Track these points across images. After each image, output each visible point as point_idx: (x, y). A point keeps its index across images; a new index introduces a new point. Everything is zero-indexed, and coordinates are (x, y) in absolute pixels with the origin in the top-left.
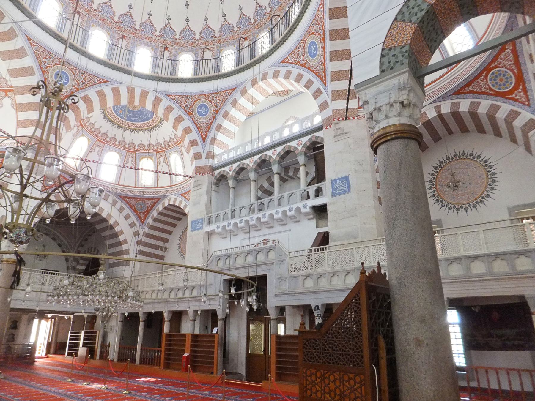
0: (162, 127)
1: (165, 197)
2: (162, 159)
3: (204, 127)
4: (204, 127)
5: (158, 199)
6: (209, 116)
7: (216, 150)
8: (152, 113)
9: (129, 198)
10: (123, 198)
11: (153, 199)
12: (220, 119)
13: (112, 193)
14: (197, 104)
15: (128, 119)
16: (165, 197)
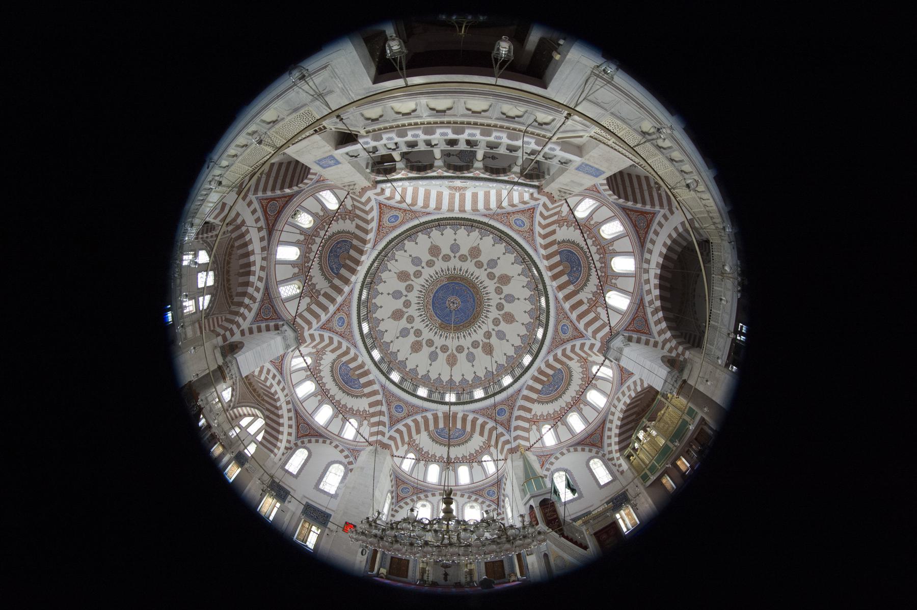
0: (566, 238)
1: (617, 205)
2: (592, 222)
3: (528, 214)
4: (528, 214)
5: (624, 209)
6: (517, 216)
7: (527, 197)
8: (560, 253)
9: (640, 238)
10: (642, 244)
11: (628, 215)
12: (510, 209)
13: (642, 256)
14: (520, 229)
15: (580, 265)
16: (617, 205)
